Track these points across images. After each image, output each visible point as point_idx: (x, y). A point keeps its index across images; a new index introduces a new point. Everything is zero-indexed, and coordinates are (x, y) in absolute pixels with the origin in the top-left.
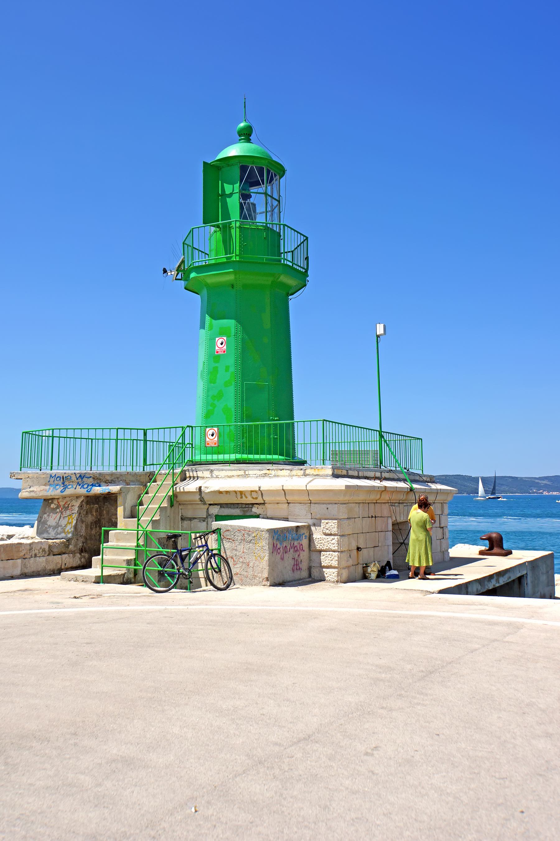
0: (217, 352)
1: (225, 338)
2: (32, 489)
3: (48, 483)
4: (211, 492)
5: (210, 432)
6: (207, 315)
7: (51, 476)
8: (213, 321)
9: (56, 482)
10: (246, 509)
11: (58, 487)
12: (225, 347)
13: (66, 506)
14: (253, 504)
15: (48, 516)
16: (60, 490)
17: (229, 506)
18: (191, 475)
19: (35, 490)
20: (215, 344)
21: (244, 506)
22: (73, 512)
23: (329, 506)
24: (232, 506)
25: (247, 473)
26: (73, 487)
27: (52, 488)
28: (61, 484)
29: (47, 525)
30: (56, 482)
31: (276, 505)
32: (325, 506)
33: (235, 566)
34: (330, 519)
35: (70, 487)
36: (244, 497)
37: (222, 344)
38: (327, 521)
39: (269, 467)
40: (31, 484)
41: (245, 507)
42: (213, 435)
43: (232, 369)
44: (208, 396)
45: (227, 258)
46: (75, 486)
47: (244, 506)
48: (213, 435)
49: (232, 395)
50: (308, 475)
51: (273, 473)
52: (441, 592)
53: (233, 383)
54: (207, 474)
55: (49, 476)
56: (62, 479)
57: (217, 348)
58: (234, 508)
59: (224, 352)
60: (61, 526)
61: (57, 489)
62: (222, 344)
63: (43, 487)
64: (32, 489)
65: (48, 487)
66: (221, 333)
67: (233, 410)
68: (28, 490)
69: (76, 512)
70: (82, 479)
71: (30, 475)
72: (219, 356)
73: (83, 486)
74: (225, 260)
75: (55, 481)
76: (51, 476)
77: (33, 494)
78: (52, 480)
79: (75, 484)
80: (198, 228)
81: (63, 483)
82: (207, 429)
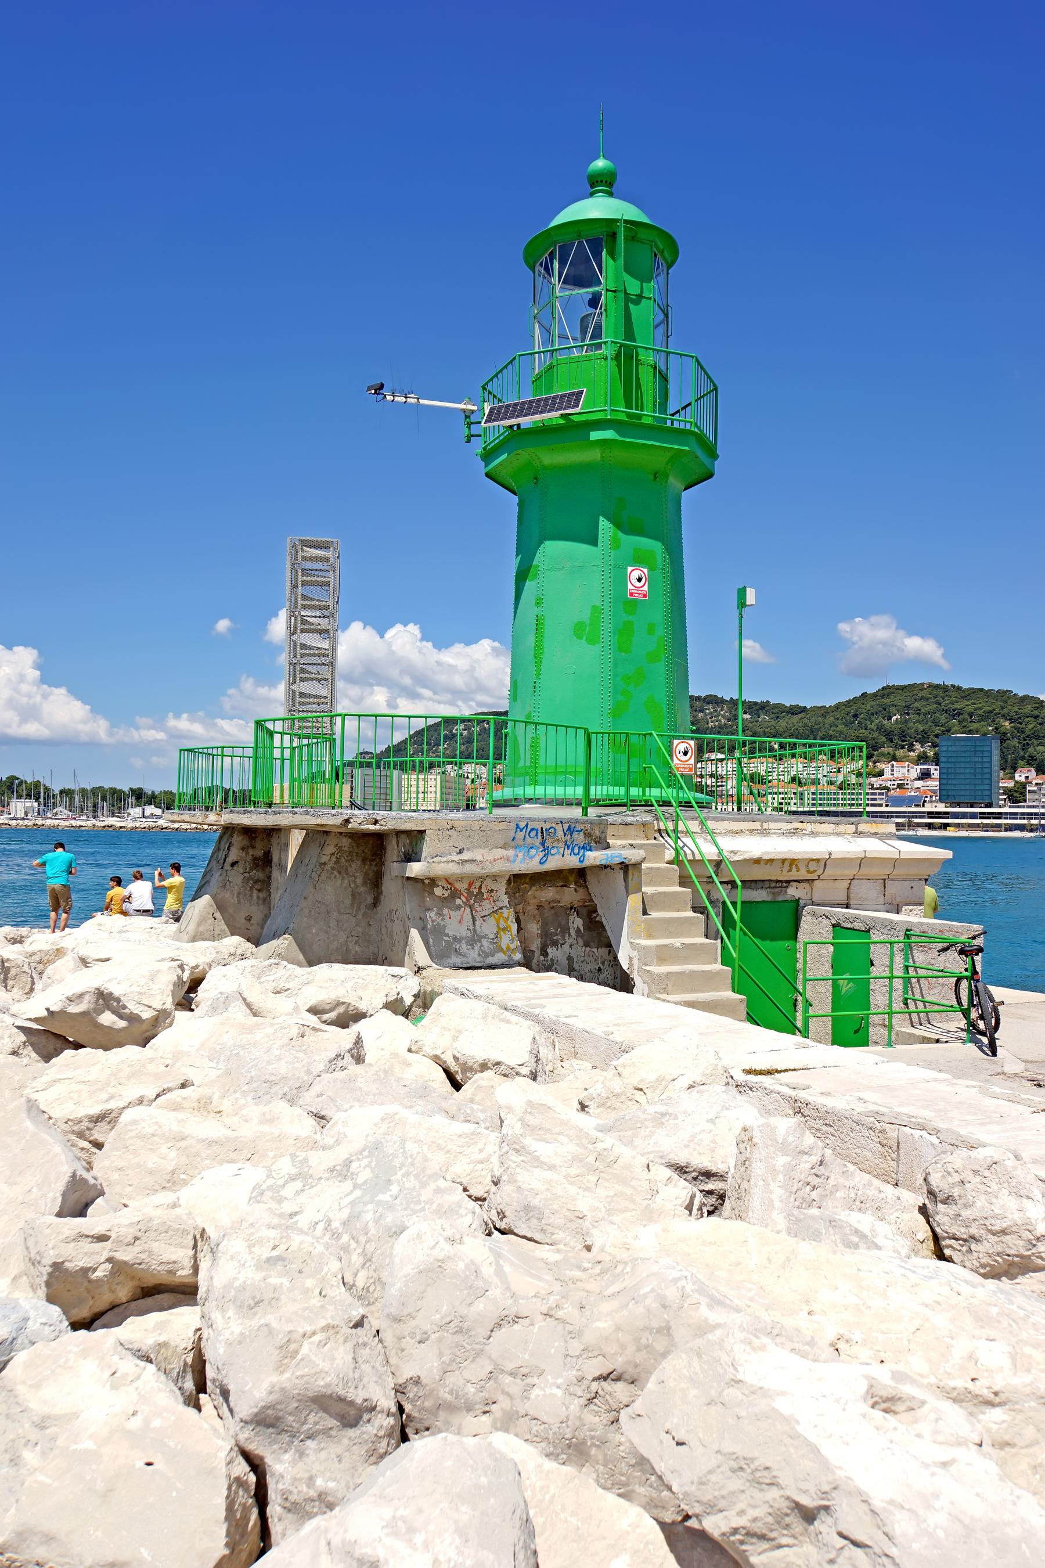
0: (631, 594)
1: (646, 571)
2: (465, 856)
3: (510, 843)
4: (745, 860)
5: (682, 747)
6: (601, 518)
7: (517, 826)
8: (620, 534)
9: (529, 840)
10: (777, 890)
11: (533, 852)
12: (646, 588)
13: (475, 891)
14: (788, 882)
15: (440, 914)
16: (537, 859)
17: (760, 885)
18: (662, 827)
19: (479, 858)
20: (625, 578)
21: (773, 885)
22: (500, 904)
23: (913, 884)
24: (753, 884)
25: (765, 826)
26: (558, 853)
27: (521, 855)
28: (538, 844)
29: (447, 935)
30: (529, 840)
31: (831, 883)
32: (908, 884)
33: (932, 992)
34: (914, 904)
35: (553, 851)
36: (794, 869)
37: (639, 580)
38: (910, 907)
39: (802, 818)
40: (461, 845)
41: (776, 887)
42: (685, 753)
43: (660, 632)
44: (616, 675)
45: (629, 415)
46: (561, 850)
47: (773, 885)
48: (685, 753)
49: (662, 679)
50: (862, 833)
51: (809, 827)
52: (676, 1003)
53: (663, 657)
54: (694, 826)
55: (513, 826)
56: (540, 834)
57: (630, 586)
58: (757, 888)
59: (645, 596)
60: (486, 936)
61: (532, 858)
62: (639, 580)
63: (500, 853)
64: (465, 856)
65: (511, 853)
66: (639, 560)
67: (664, 706)
68: (456, 858)
69: (506, 903)
70: (571, 834)
71: (456, 824)
72: (636, 601)
73: (573, 849)
74: (623, 417)
75: (528, 839)
76: (517, 826)
77: (470, 868)
78: (520, 835)
79: (562, 845)
80: (681, 355)
81: (543, 844)
82: (676, 742)
